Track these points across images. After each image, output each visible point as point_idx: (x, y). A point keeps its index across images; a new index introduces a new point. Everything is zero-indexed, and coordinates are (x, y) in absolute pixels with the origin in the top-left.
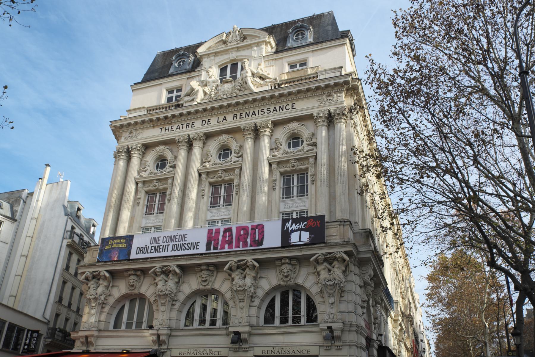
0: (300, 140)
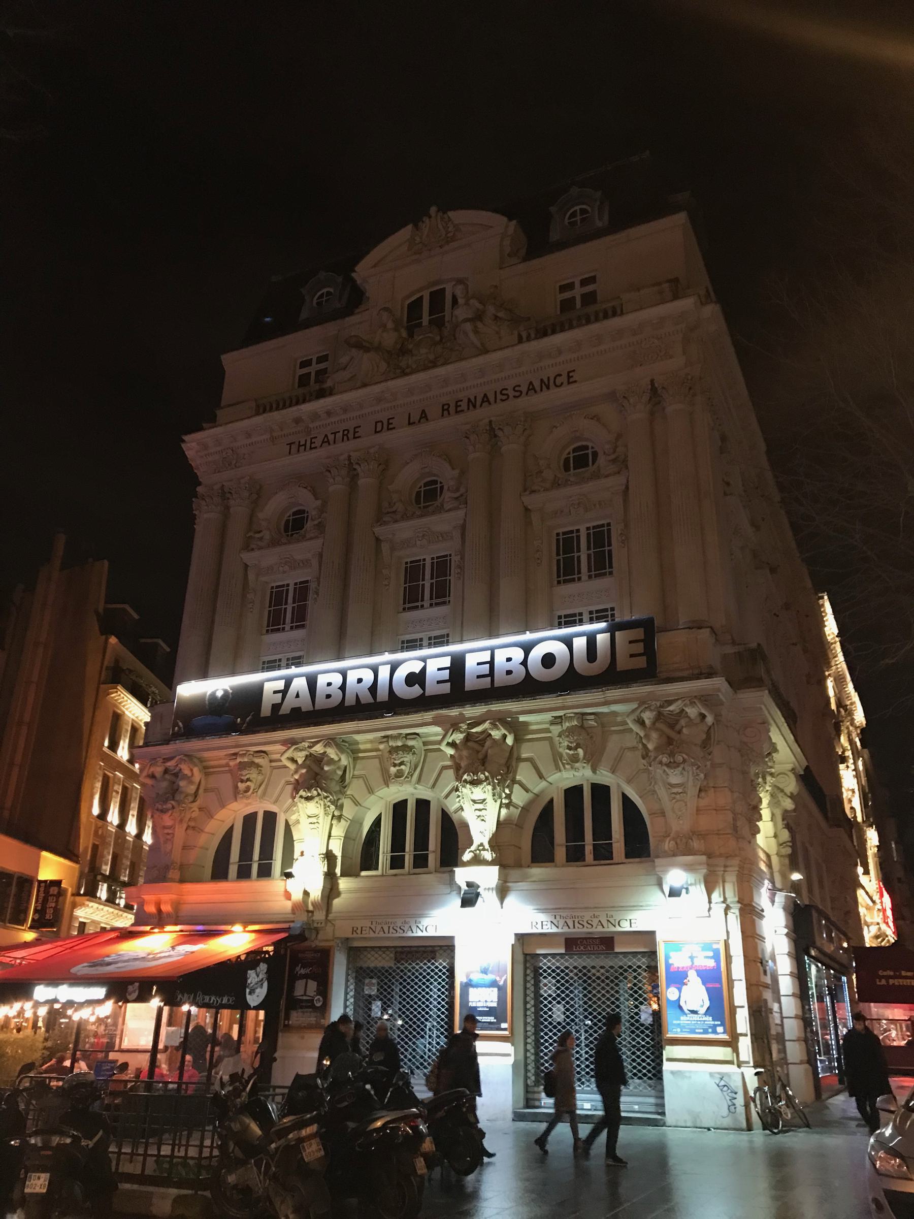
0: (590, 451)
